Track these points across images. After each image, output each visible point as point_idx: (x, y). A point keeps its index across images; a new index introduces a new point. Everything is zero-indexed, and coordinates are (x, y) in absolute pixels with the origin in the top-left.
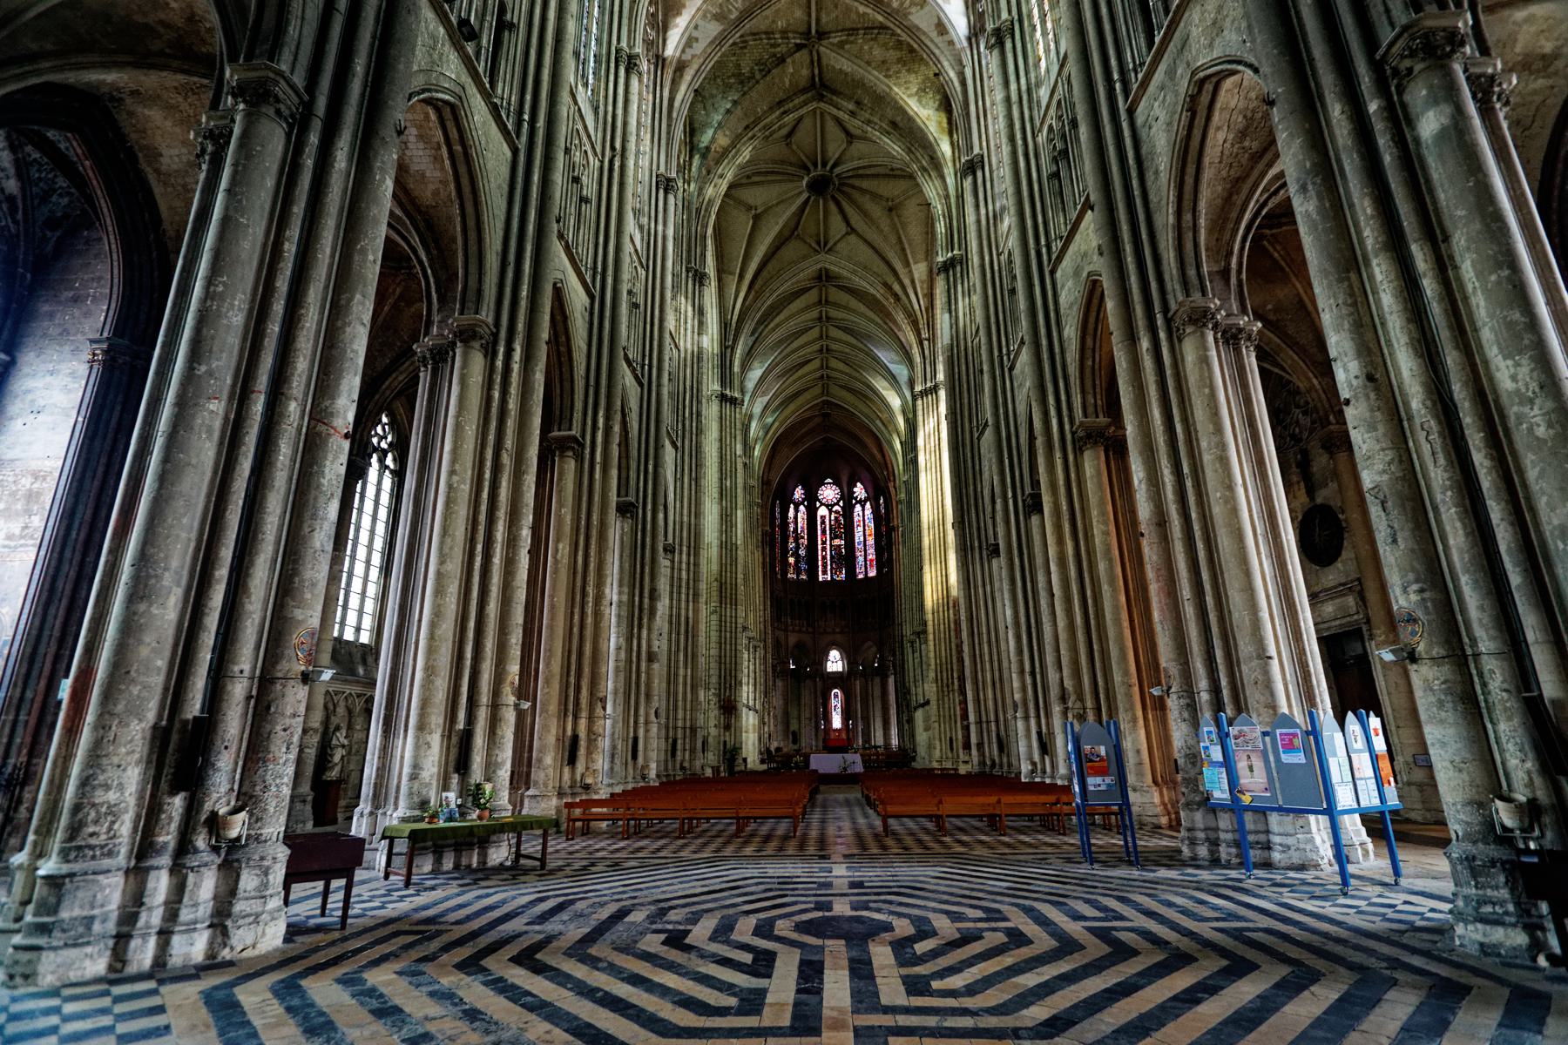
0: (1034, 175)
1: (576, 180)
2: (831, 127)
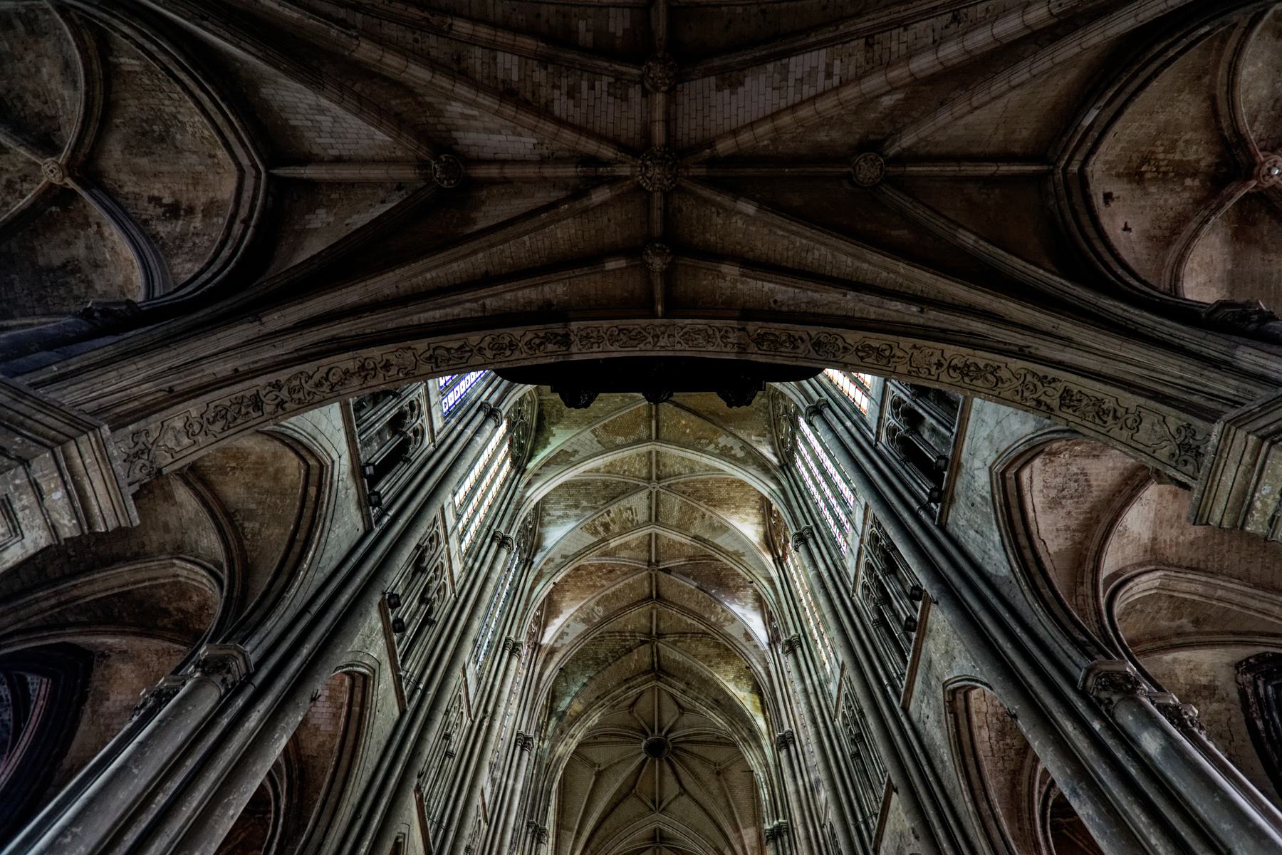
0: (839, 754)
1: (447, 737)
2: (666, 700)
